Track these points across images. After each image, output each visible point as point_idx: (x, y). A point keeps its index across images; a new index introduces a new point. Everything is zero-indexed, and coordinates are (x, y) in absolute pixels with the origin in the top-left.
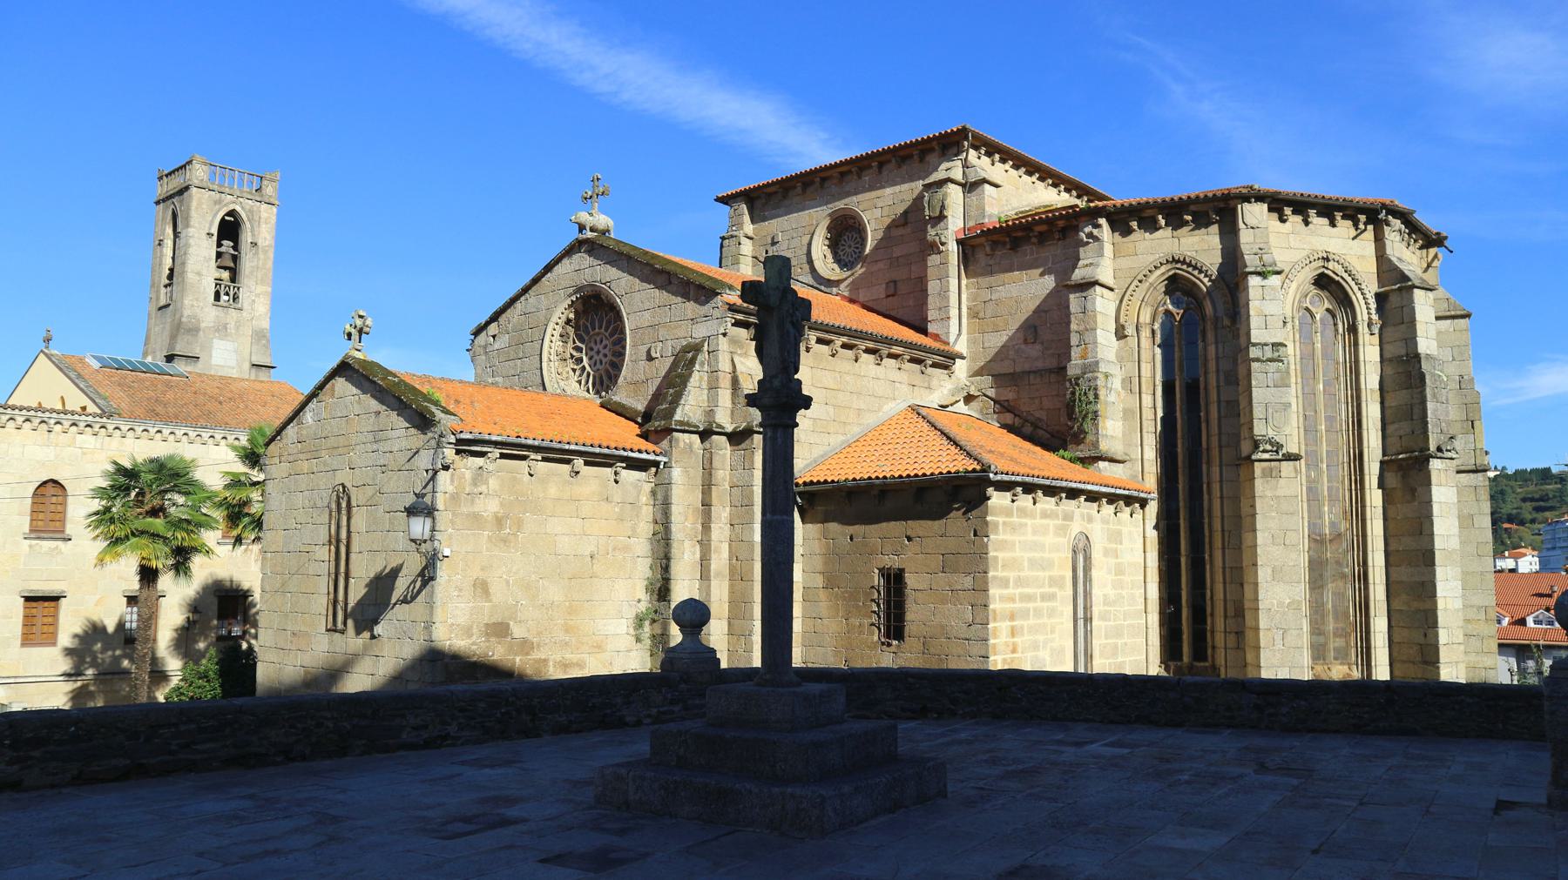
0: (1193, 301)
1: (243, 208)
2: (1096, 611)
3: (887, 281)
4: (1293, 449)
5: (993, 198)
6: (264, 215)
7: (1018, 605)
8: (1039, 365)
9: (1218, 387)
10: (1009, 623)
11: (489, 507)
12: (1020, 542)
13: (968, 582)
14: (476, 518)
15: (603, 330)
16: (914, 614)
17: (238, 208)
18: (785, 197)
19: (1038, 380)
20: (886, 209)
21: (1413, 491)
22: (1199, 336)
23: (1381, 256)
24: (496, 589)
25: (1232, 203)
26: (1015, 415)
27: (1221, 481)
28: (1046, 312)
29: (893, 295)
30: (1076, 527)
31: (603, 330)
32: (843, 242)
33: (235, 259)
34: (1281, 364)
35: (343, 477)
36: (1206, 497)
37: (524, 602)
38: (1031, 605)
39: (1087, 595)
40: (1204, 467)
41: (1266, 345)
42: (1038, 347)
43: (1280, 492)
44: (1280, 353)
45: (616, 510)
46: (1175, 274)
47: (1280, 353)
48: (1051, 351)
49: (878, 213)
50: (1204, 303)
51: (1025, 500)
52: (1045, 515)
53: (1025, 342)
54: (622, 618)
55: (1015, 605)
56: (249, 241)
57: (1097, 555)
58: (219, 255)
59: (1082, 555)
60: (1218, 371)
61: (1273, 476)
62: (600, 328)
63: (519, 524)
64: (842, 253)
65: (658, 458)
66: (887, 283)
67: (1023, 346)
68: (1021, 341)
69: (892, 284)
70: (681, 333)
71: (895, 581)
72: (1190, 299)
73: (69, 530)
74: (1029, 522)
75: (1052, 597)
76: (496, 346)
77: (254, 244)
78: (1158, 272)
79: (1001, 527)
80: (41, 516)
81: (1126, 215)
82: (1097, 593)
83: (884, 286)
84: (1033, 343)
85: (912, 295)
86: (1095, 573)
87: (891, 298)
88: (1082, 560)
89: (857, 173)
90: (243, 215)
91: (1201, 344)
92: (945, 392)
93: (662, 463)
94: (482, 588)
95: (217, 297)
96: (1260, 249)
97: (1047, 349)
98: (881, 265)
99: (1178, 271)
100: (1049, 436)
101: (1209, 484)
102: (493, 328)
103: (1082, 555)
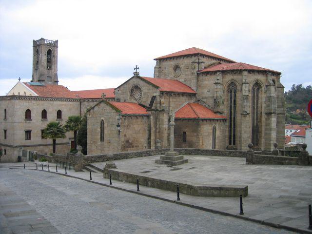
4: (248, 112)
11: (126, 124)
13: (195, 134)
14: (124, 126)
16: (188, 138)
18: (166, 60)
21: (269, 119)
23: (267, 79)
24: (127, 136)
33: (50, 59)
35: (102, 118)
39: (215, 135)
51: (205, 122)
57: (217, 128)
58: (47, 59)
59: (214, 130)
63: (130, 126)
71: (185, 133)
73: (32, 118)
86: (216, 132)
94: (125, 136)
95: (47, 67)
102: (118, 89)
103: (214, 130)
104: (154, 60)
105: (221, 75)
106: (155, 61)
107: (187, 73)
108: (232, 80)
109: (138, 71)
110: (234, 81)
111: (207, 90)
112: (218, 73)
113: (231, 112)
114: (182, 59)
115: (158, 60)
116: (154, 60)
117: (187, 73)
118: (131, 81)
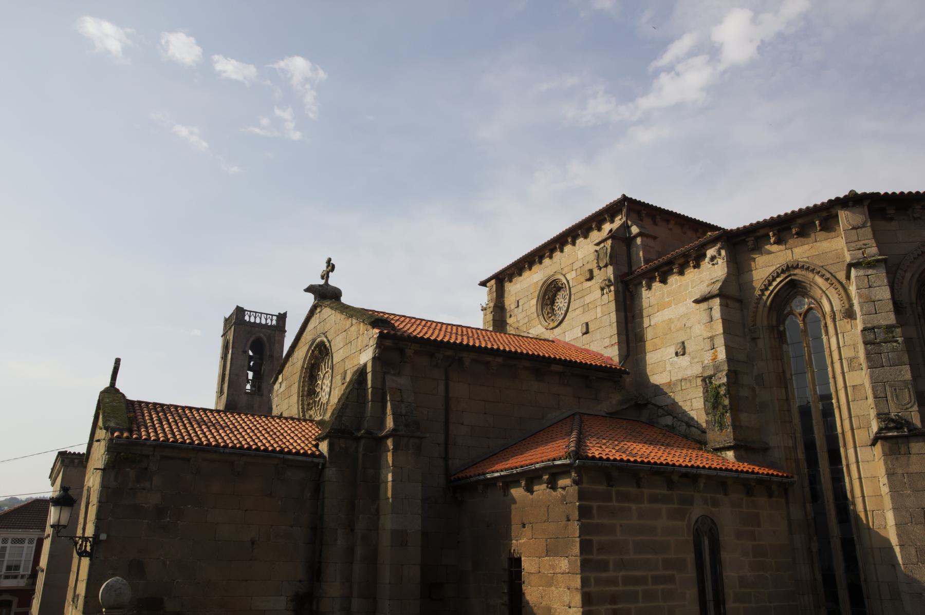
0: (813, 301)
1: (265, 335)
2: (729, 592)
3: (581, 323)
5: (650, 247)
6: (277, 338)
7: (621, 588)
8: (689, 373)
9: (843, 373)
10: (609, 607)
12: (621, 526)
15: (329, 369)
17: (262, 335)
19: (688, 384)
20: (579, 270)
22: (823, 331)
25: (833, 211)
26: (674, 417)
27: (857, 462)
28: (691, 327)
29: (587, 332)
30: (697, 511)
31: (329, 369)
32: (557, 301)
34: (895, 344)
36: (847, 479)
37: (180, 581)
38: (640, 588)
40: (842, 450)
41: (879, 327)
42: (686, 357)
43: (911, 470)
44: (894, 334)
45: (280, 503)
46: (791, 279)
47: (894, 334)
48: (696, 360)
49: (574, 274)
50: (822, 301)
52: (653, 499)
53: (677, 354)
54: (281, 595)
55: (617, 589)
56: (268, 353)
57: (728, 537)
60: (841, 359)
61: (903, 452)
62: (328, 368)
64: (556, 309)
65: (316, 460)
66: (582, 325)
67: (676, 359)
68: (674, 355)
69: (584, 325)
70: (356, 363)
72: (810, 300)
74: (634, 506)
75: (670, 579)
76: (281, 390)
77: (271, 356)
78: (779, 280)
79: (595, 511)
80: (44, 521)
81: (744, 237)
82: (730, 575)
83: (581, 326)
84: (682, 355)
85: (598, 331)
87: (585, 335)
88: (706, 542)
89: (559, 248)
90: (265, 339)
91: (824, 338)
92: (614, 402)
93: (321, 464)
96: (864, 245)
97: (693, 358)
98: (578, 312)
99: (793, 277)
100: (699, 432)
101: (848, 466)
104: (483, 284)
105: (723, 252)
106: (485, 290)
107: (587, 299)
108: (788, 268)
109: (334, 281)
110: (799, 274)
111: (672, 350)
112: (710, 252)
113: (810, 447)
114: (568, 248)
115: (493, 282)
116: (483, 284)
117: (587, 299)
118: (311, 326)
